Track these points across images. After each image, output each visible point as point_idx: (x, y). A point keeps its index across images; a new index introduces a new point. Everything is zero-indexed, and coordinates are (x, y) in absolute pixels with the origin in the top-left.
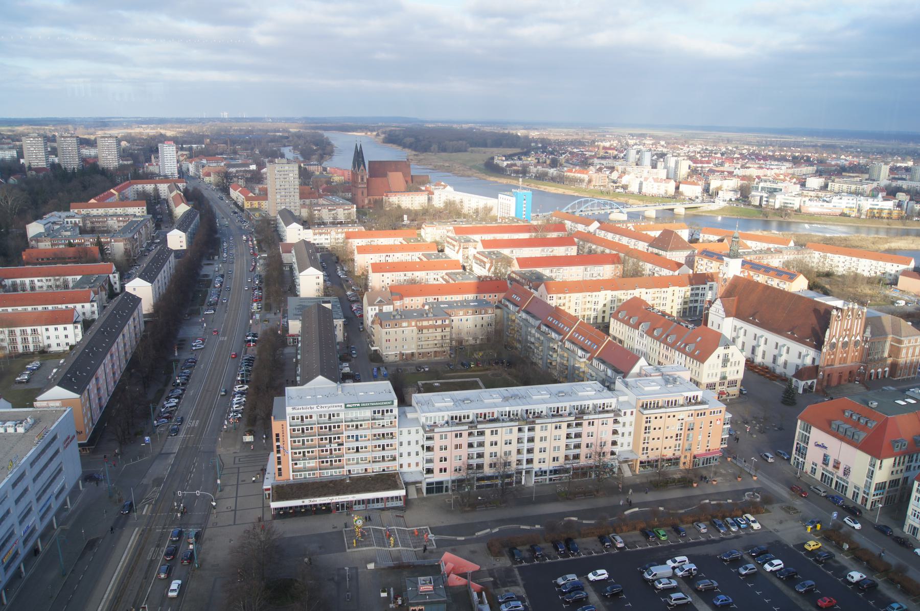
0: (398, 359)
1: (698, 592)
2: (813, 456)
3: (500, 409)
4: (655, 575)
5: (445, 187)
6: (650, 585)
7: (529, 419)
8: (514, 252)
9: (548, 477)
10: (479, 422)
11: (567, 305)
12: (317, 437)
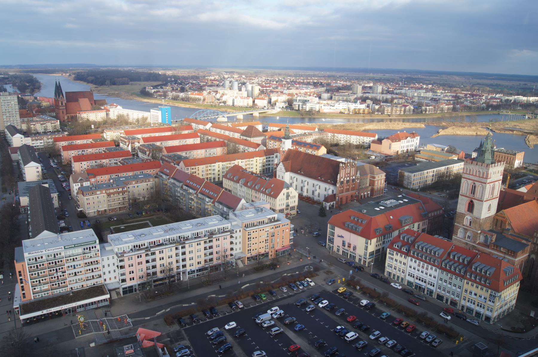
0: (96, 214)
1: (286, 325)
2: (338, 242)
3: (163, 238)
4: (262, 320)
5: (116, 106)
6: (260, 326)
7: (181, 242)
8: (163, 143)
9: (196, 274)
10: (152, 247)
11: (197, 172)
12: (47, 270)
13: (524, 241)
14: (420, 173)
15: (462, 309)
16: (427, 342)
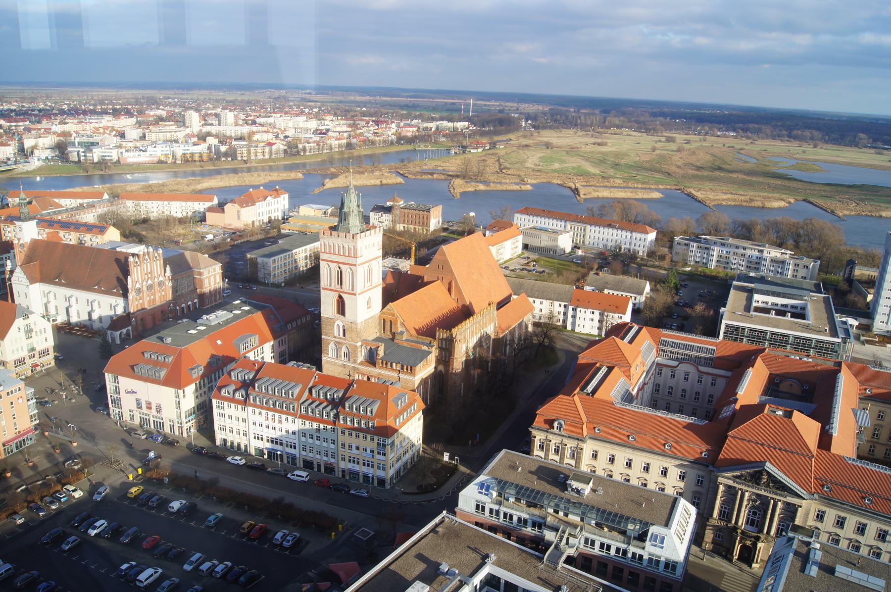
13: (425, 348)
14: (282, 255)
15: (344, 476)
16: (286, 549)
